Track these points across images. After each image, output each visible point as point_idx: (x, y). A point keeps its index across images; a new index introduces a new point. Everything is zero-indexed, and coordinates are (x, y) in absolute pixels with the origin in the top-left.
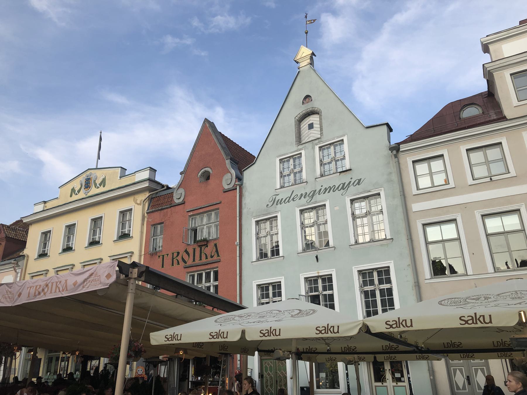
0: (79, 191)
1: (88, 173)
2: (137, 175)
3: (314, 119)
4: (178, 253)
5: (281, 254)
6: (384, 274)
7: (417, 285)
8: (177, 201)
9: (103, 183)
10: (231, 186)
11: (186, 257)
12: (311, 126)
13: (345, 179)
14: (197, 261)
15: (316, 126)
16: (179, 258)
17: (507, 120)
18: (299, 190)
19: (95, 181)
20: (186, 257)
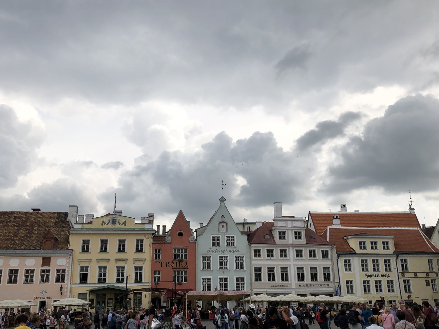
0: (108, 224)
1: (114, 216)
2: (145, 225)
3: (224, 225)
4: (169, 263)
5: (212, 269)
6: (243, 279)
7: (251, 283)
8: (168, 242)
10: (193, 241)
12: (223, 226)
13: (234, 249)
14: (178, 266)
15: (225, 227)
16: (170, 264)
17: (276, 244)
18: (218, 249)
19: (118, 221)
20: (173, 265)
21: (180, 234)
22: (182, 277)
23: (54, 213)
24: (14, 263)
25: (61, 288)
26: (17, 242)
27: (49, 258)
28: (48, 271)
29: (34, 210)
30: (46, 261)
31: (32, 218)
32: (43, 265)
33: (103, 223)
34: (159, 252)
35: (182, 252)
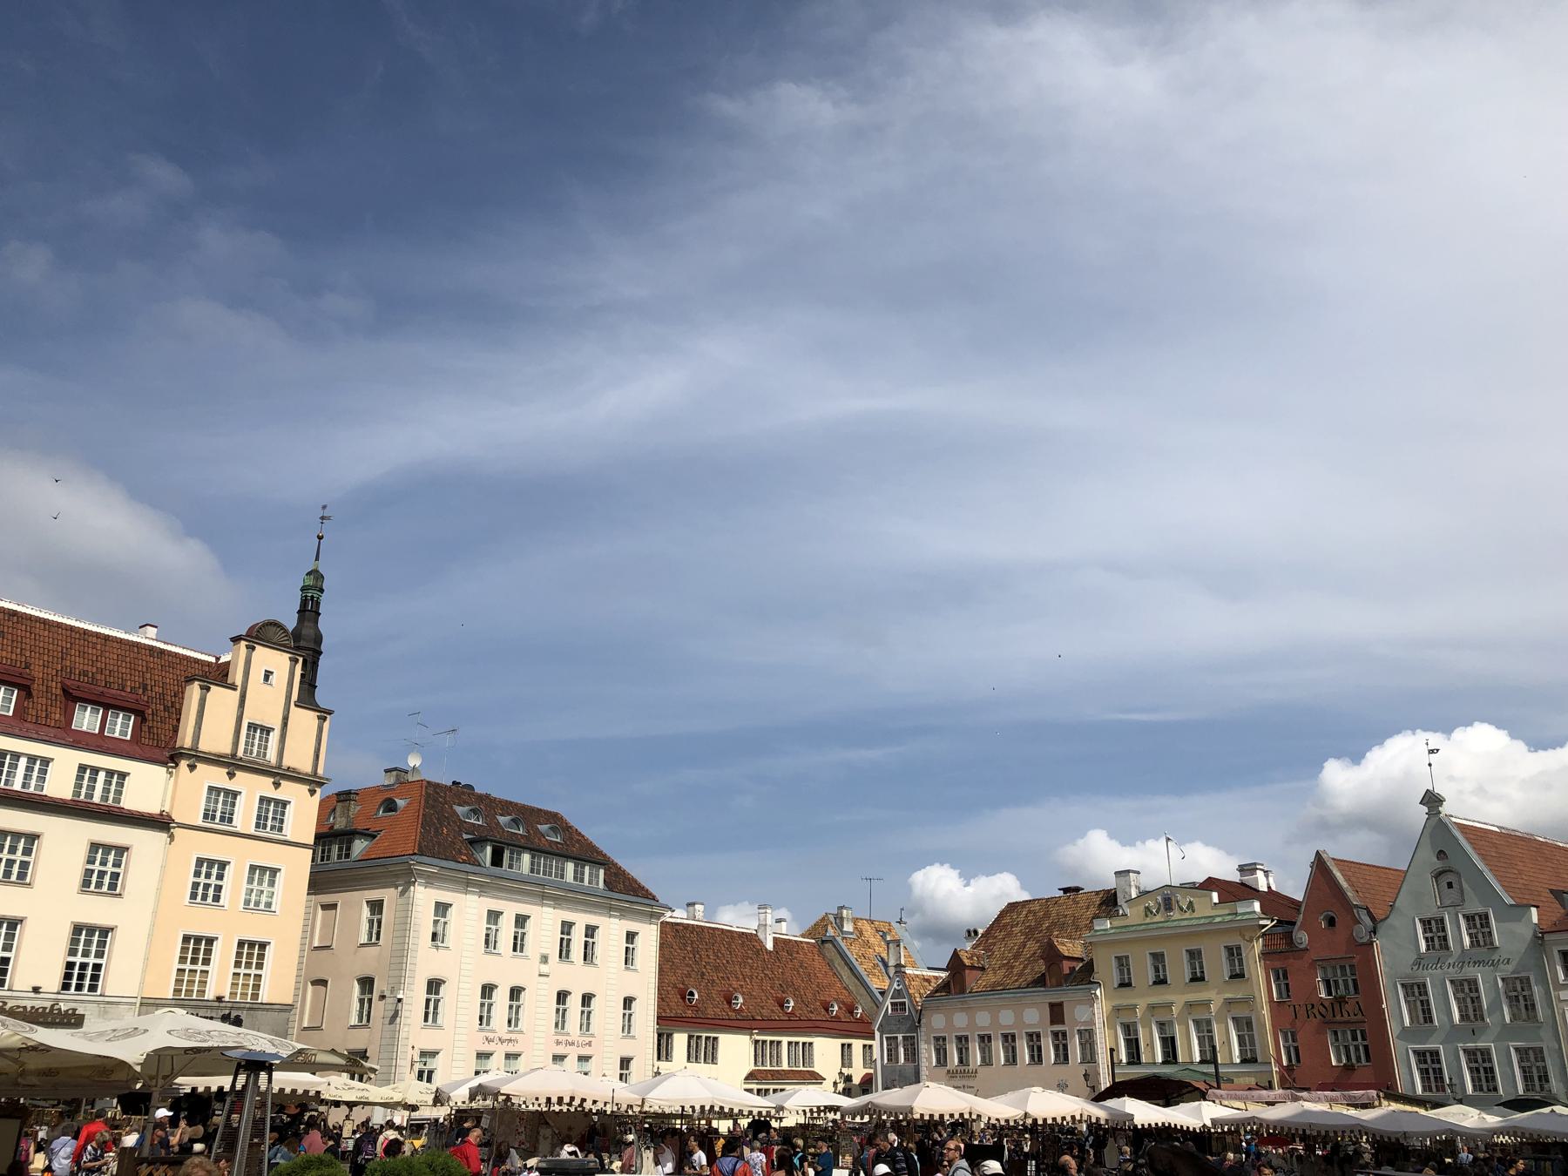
9: (1191, 905)
11: (1323, 1010)
12: (1450, 885)
14: (1338, 1018)
20: (1323, 1010)
21: (1331, 922)
22: (1357, 1048)
23: (1097, 893)
24: (1007, 1018)
25: (1086, 1076)
26: (1015, 971)
27: (1061, 1005)
28: (1064, 1034)
29: (1066, 890)
30: (1057, 1013)
31: (1054, 911)
32: (1053, 1022)
33: (1148, 909)
34: (1285, 977)
35: (1344, 974)
